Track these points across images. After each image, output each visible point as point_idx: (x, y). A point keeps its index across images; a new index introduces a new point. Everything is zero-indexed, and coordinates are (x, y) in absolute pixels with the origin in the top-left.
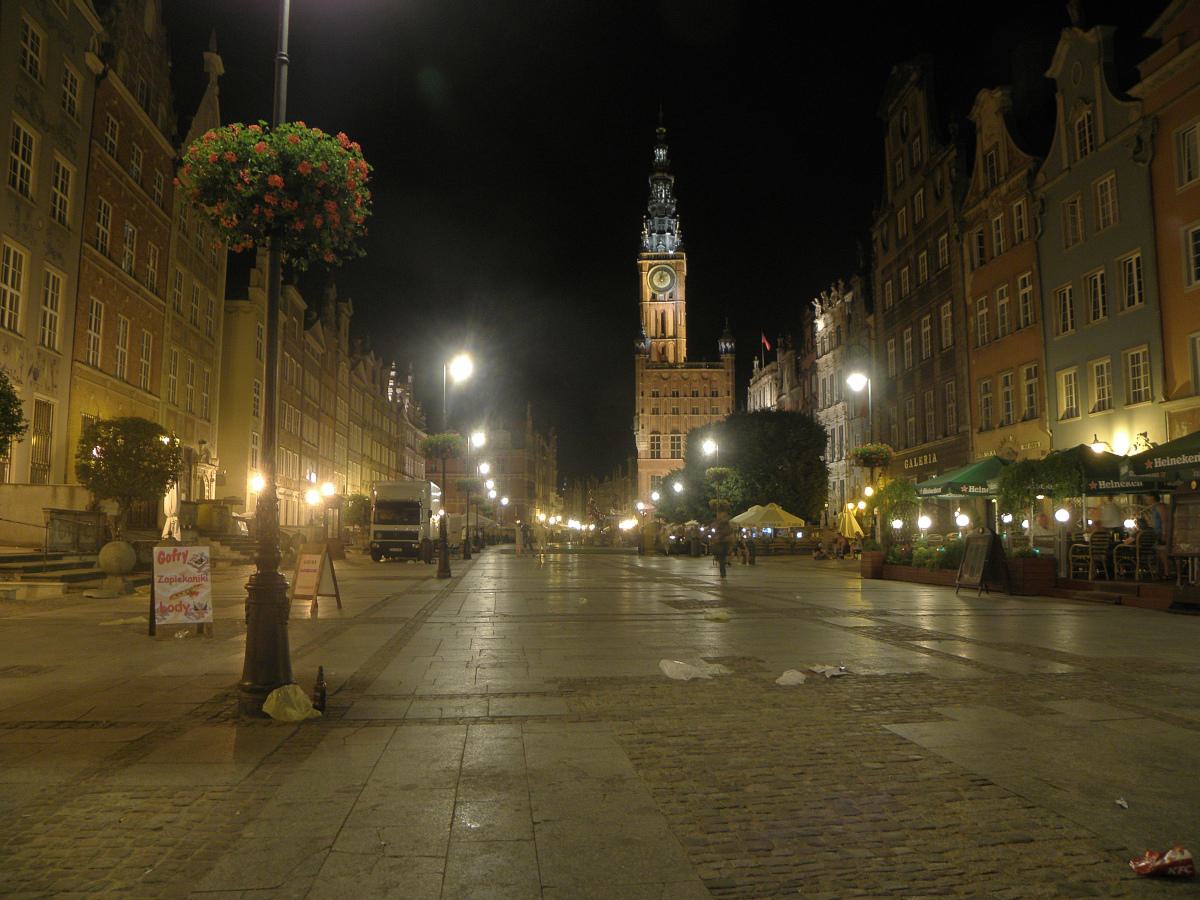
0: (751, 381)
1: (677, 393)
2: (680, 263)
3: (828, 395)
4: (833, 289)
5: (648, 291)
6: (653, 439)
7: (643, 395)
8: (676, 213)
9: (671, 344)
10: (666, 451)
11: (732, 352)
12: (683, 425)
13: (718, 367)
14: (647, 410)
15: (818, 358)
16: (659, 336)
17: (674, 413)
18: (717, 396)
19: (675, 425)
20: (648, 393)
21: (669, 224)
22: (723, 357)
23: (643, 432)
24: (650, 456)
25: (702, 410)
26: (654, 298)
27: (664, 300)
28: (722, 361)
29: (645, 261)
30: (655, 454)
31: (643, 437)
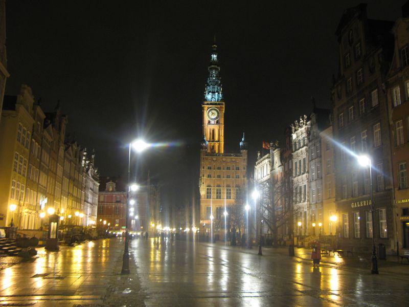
0: (257, 163)
2: (222, 107)
3: (298, 170)
4: (301, 119)
6: (208, 189)
8: (220, 84)
9: (217, 145)
10: (214, 195)
14: (205, 175)
15: (293, 152)
16: (211, 140)
17: (218, 177)
19: (219, 183)
20: (206, 167)
22: (242, 151)
26: (209, 122)
27: (212, 122)
28: (241, 153)
30: (208, 196)
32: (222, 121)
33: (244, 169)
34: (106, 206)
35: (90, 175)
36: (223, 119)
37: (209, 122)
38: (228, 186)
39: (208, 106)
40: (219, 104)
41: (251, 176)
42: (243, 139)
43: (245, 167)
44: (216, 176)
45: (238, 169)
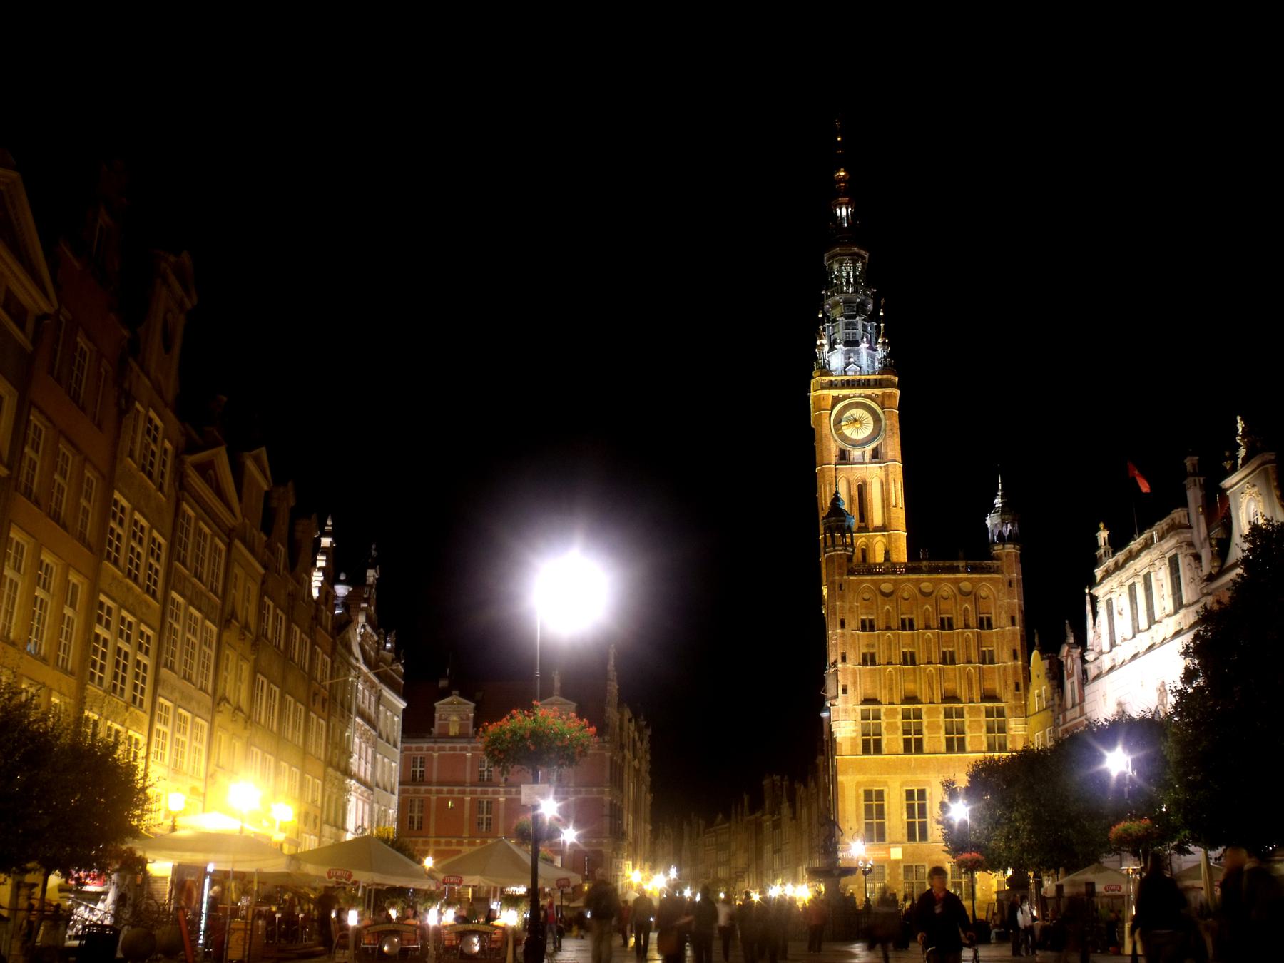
0: (1098, 573)
1: (911, 621)
2: (890, 395)
5: (830, 446)
7: (843, 625)
10: (893, 739)
11: (1012, 539)
12: (925, 687)
13: (988, 570)
17: (905, 663)
18: (990, 627)
19: (910, 687)
20: (853, 623)
21: (865, 330)
22: (998, 549)
23: (846, 702)
24: (860, 748)
25: (960, 656)
27: (861, 453)
28: (998, 558)
29: (825, 392)
30: (871, 745)
31: (846, 711)
32: (893, 448)
33: (1013, 624)
34: (434, 798)
35: (357, 651)
36: (897, 439)
37: (843, 457)
38: (950, 698)
39: (835, 393)
40: (878, 384)
41: (1063, 639)
42: (998, 502)
43: (1018, 617)
44: (897, 657)
45: (985, 623)
